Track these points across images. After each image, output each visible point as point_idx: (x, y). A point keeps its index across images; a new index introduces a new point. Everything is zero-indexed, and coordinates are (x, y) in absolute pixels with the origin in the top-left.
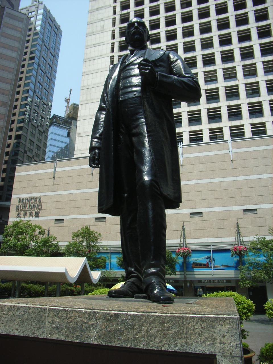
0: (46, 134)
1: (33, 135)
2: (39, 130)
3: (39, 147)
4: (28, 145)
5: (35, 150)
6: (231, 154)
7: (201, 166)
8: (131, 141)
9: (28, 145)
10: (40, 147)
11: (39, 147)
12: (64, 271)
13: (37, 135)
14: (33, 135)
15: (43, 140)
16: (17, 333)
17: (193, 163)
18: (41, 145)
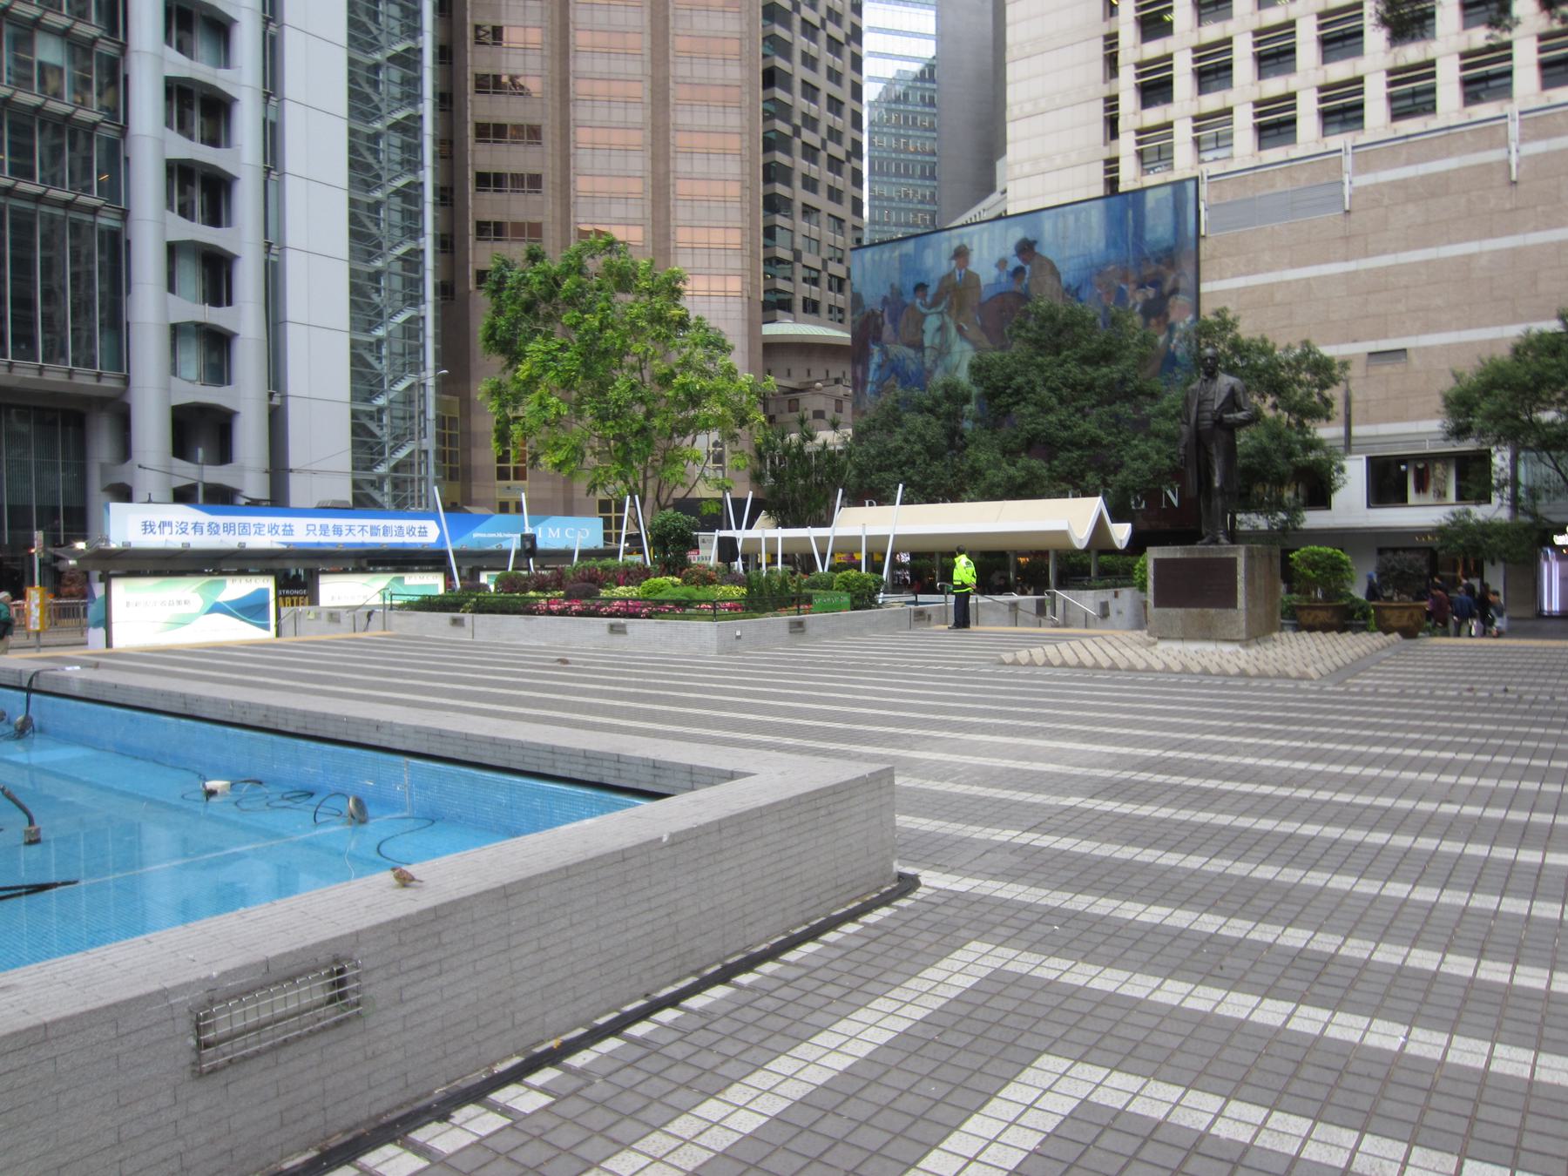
0: (854, 46)
1: (810, 61)
2: (829, 36)
3: (835, 105)
4: (801, 104)
5: (827, 118)
6: (1514, 160)
7: (1411, 209)
9: (801, 104)
10: (842, 103)
11: (835, 105)
13: (826, 59)
14: (810, 61)
15: (849, 75)
17: (1386, 201)
18: (844, 94)
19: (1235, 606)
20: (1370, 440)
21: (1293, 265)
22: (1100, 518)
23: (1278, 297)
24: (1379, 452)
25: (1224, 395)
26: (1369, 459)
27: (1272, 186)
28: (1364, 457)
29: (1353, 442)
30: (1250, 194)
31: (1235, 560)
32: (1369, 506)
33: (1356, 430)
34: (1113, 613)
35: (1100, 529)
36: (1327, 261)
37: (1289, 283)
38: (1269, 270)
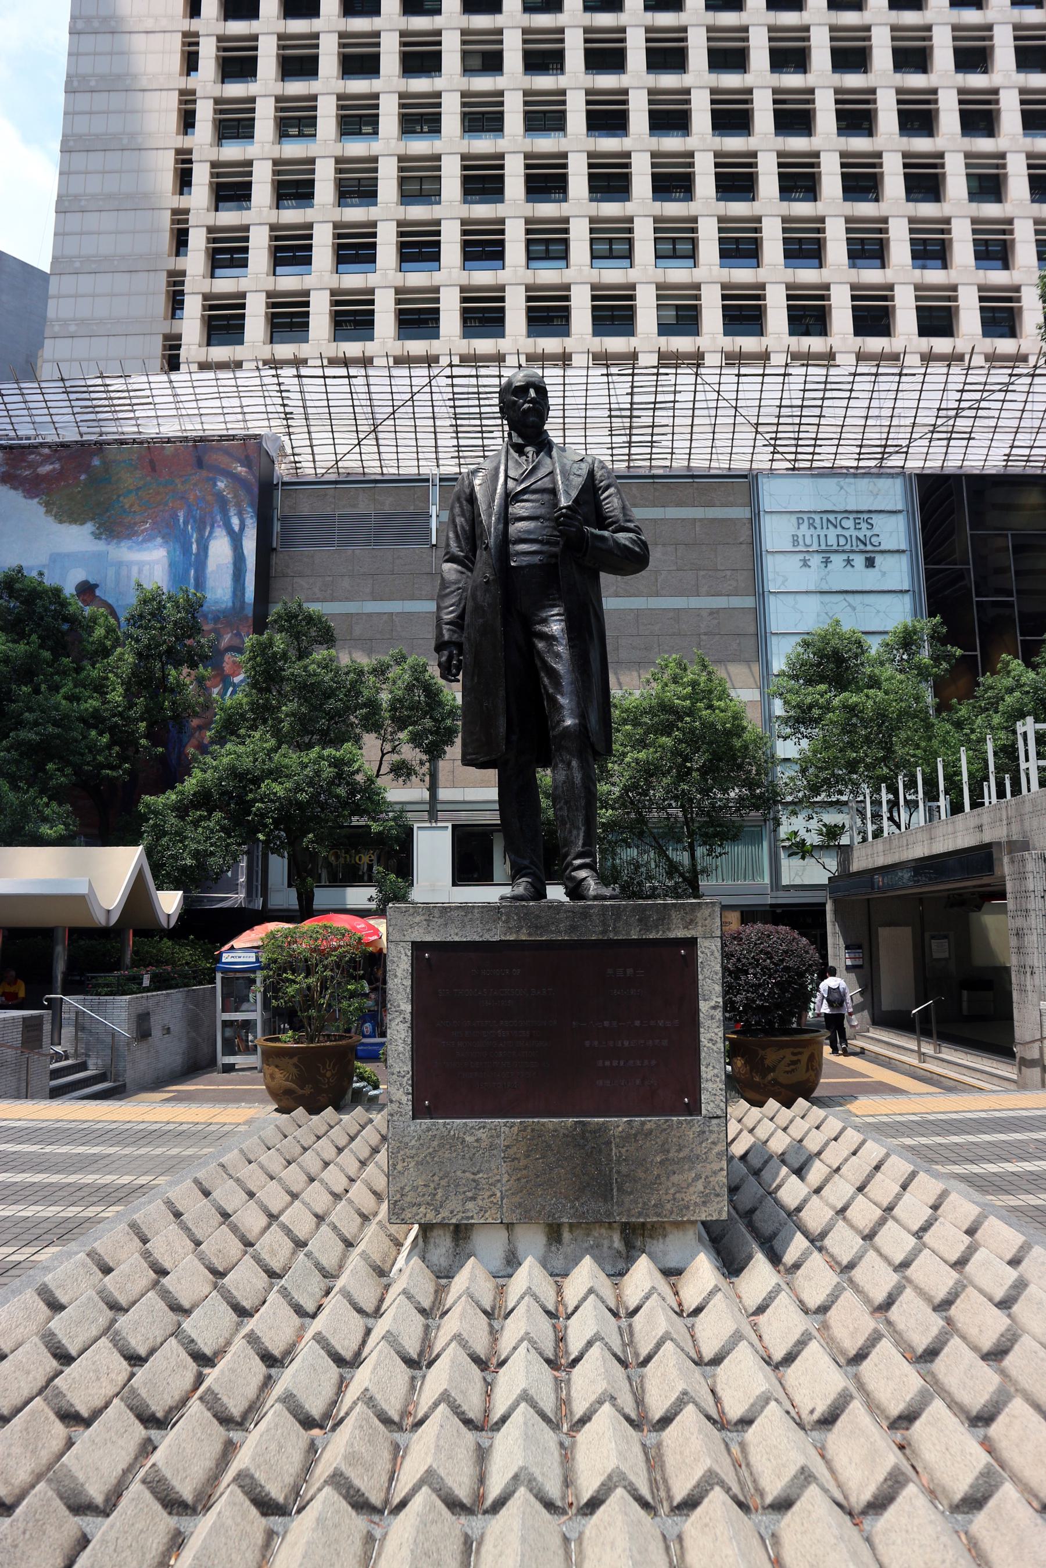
8: (534, 646)
12: (83, 890)
16: (457, 939)
19: (694, 1108)
20: (457, 806)
21: (375, 597)
22: (139, 880)
23: (357, 631)
24: (465, 818)
25: (578, 482)
26: (455, 827)
27: (354, 506)
28: (449, 825)
29: (439, 807)
30: (328, 511)
31: (691, 943)
32: (454, 884)
33: (443, 794)
34: (156, 1032)
35: (138, 897)
36: (412, 598)
37: (370, 615)
38: (347, 599)
